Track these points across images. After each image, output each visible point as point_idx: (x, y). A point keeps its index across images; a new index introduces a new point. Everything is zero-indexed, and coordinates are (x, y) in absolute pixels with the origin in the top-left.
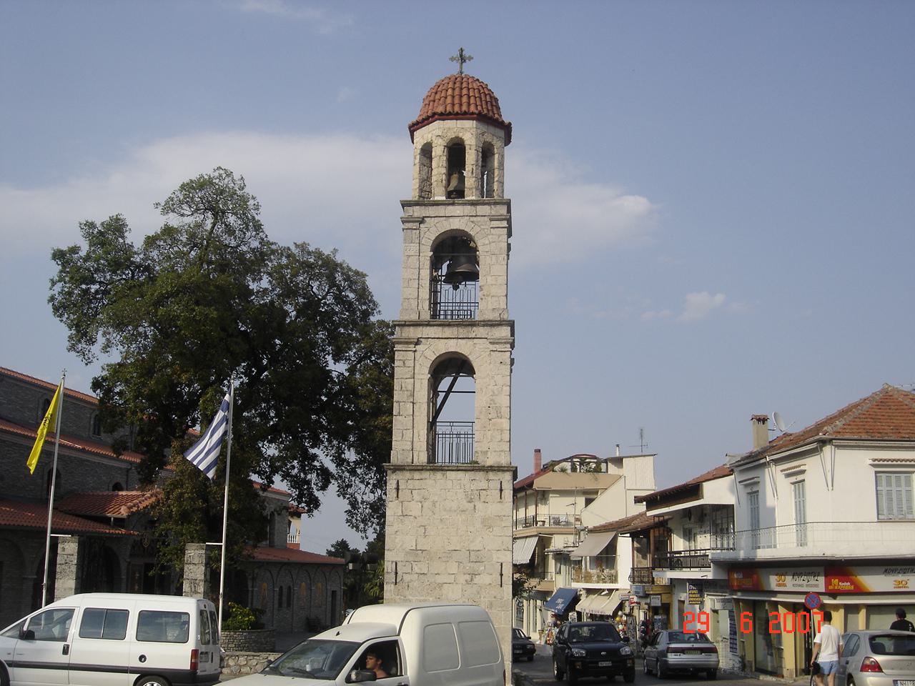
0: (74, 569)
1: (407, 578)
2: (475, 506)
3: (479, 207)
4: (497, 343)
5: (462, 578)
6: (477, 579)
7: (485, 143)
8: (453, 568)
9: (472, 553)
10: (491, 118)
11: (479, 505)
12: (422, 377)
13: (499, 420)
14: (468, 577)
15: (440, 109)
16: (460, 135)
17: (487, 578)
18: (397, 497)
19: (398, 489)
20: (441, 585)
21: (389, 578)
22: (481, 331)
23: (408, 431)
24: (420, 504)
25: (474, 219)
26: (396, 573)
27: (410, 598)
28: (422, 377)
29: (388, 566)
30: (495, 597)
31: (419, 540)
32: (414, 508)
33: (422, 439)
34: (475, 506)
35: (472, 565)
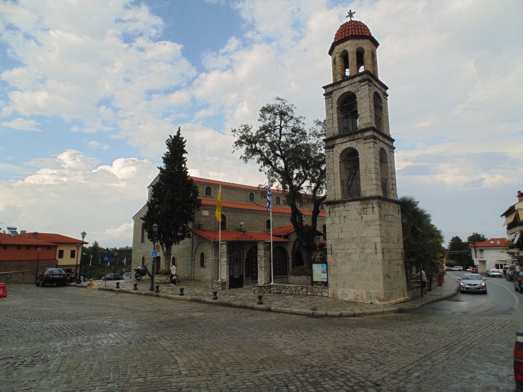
0: (226, 254)
1: (336, 251)
2: (362, 217)
3: (355, 79)
4: (367, 139)
5: (359, 250)
7: (358, 49)
8: (355, 247)
9: (362, 239)
10: (359, 36)
11: (364, 216)
12: (336, 161)
13: (371, 175)
14: (361, 250)
16: (345, 49)
17: (370, 250)
18: (330, 216)
19: (329, 212)
21: (329, 252)
23: (333, 186)
24: (339, 218)
25: (354, 85)
26: (331, 250)
27: (338, 260)
28: (336, 161)
29: (328, 247)
30: (374, 259)
31: (339, 234)
32: (337, 220)
33: (339, 189)
34: (362, 217)
35: (363, 244)
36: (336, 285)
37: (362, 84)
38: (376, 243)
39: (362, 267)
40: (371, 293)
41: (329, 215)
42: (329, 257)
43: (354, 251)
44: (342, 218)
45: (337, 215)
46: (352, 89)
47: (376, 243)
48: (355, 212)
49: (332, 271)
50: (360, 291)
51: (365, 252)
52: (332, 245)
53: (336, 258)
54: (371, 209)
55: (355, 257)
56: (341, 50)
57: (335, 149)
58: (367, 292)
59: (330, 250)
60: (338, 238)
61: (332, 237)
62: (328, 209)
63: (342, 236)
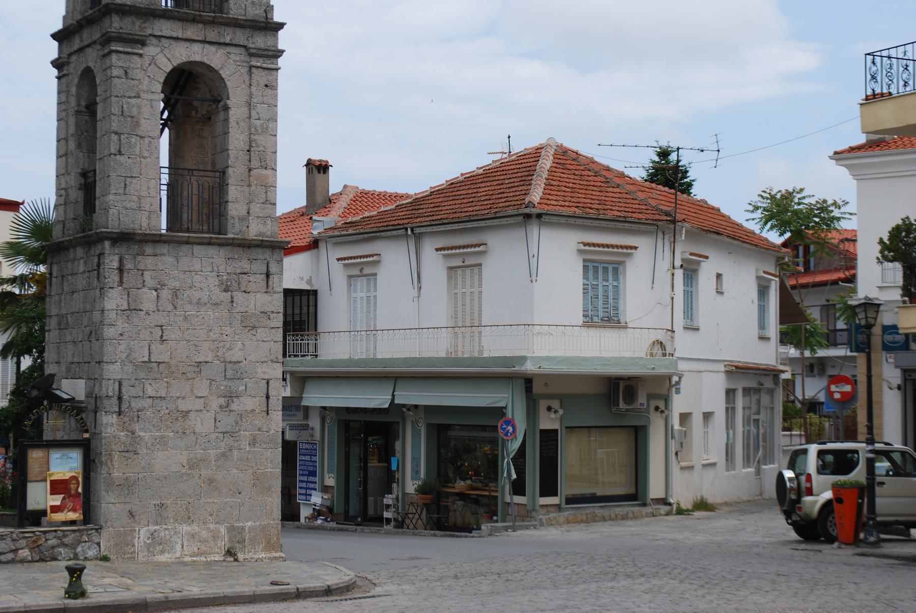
1: (137, 404)
5: (215, 403)
11: (239, 297)
14: (222, 401)
18: (121, 283)
19: (121, 270)
24: (155, 293)
26: (120, 398)
27: (142, 434)
31: (153, 347)
32: (147, 298)
36: (131, 514)
38: (268, 383)
39: (223, 455)
40: (243, 528)
41: (117, 279)
43: (199, 404)
45: (149, 282)
47: (268, 383)
48: (213, 281)
50: (212, 526)
51: (234, 407)
52: (125, 384)
53: (136, 427)
54: (263, 276)
55: (203, 424)
58: (231, 529)
59: (115, 401)
60: (146, 359)
61: (124, 356)
62: (116, 258)
63: (161, 353)
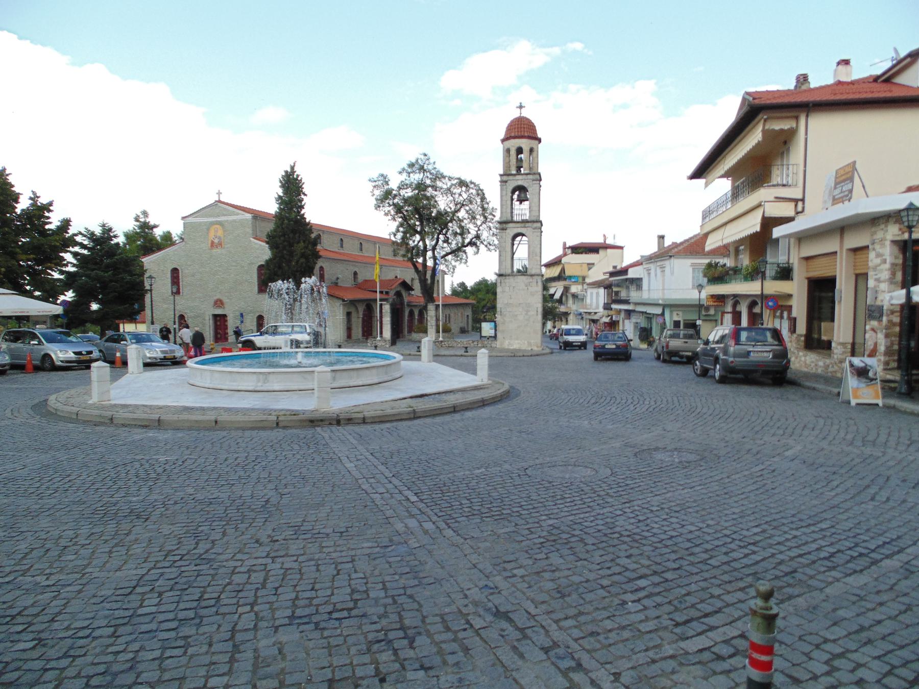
6: (529, 313)
8: (521, 310)
15: (513, 135)
17: (533, 313)
20: (516, 316)
22: (530, 224)
29: (498, 309)
32: (507, 289)
37: (534, 182)
42: (499, 318)
44: (511, 288)
46: (526, 185)
49: (499, 328)
56: (518, 146)
57: (507, 231)
58: (528, 342)
